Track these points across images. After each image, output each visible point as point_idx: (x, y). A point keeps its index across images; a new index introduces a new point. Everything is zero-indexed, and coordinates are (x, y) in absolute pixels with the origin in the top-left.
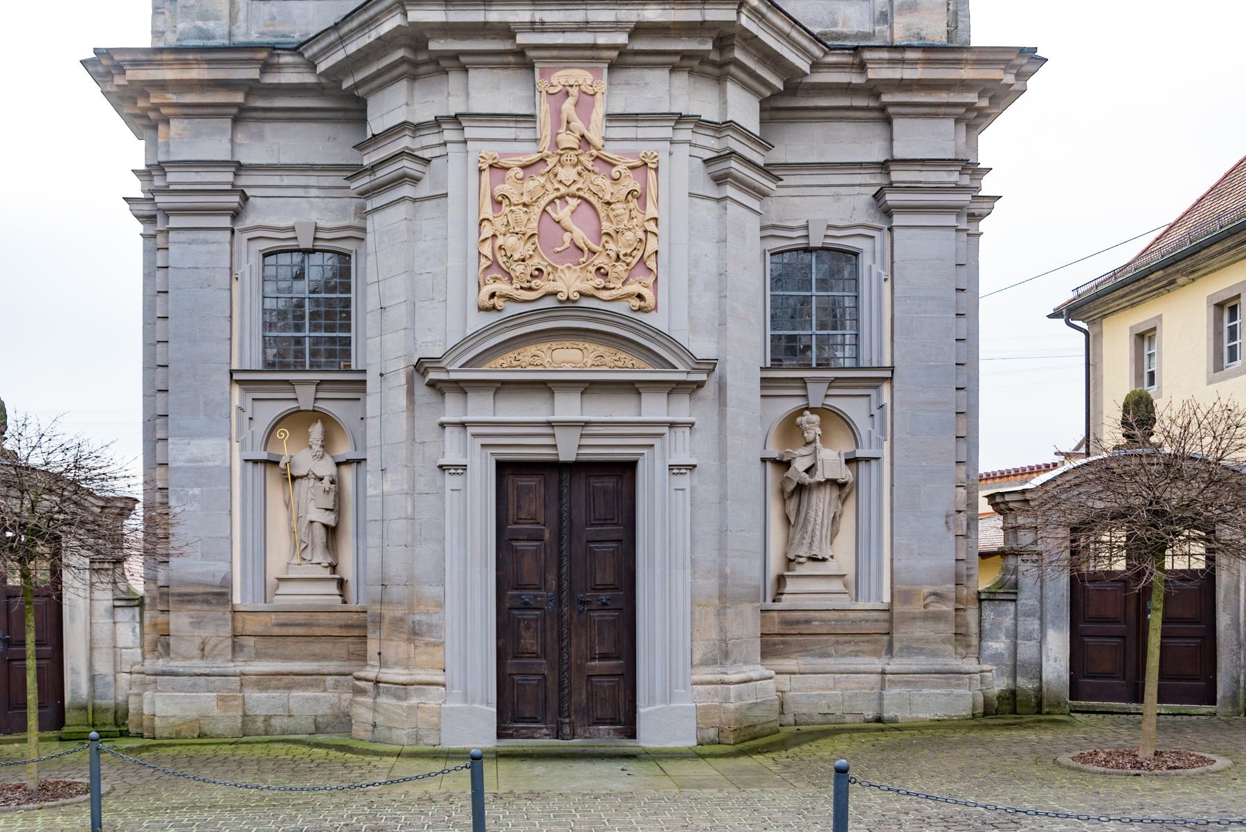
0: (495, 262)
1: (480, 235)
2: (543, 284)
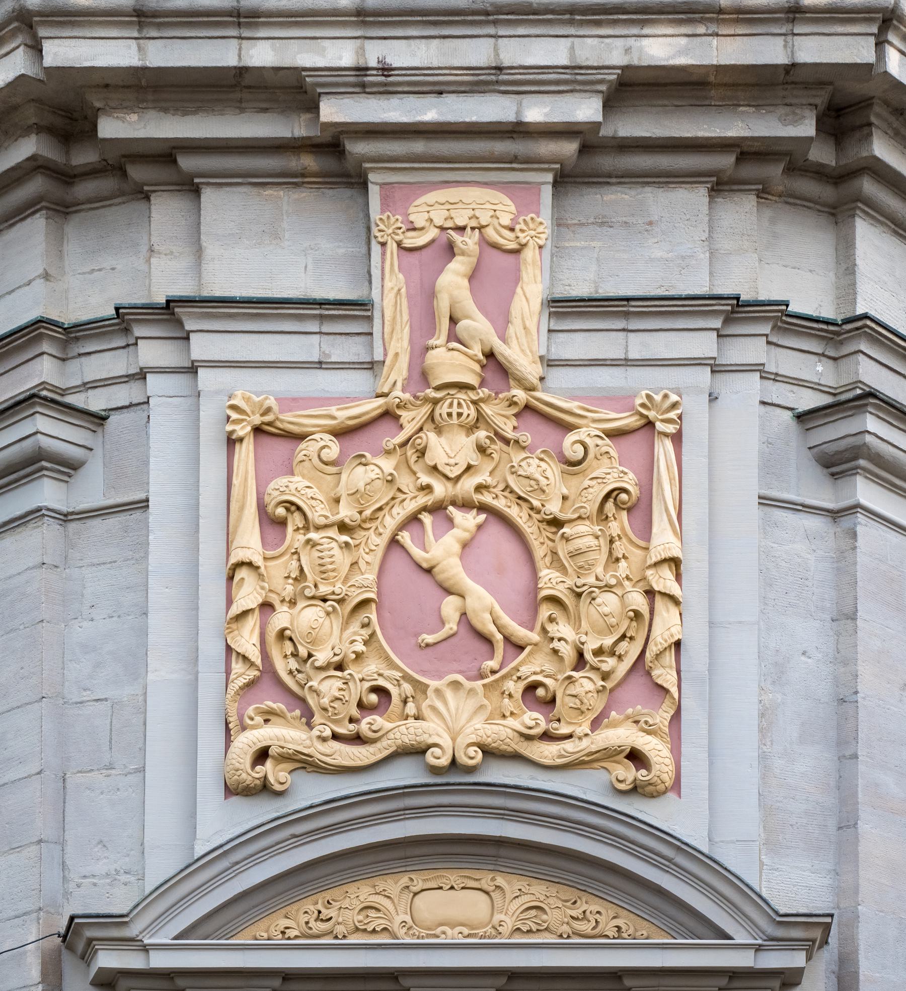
0: (268, 670)
1: (229, 602)
2: (388, 725)
